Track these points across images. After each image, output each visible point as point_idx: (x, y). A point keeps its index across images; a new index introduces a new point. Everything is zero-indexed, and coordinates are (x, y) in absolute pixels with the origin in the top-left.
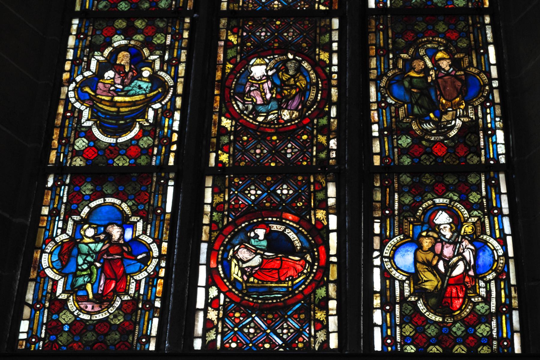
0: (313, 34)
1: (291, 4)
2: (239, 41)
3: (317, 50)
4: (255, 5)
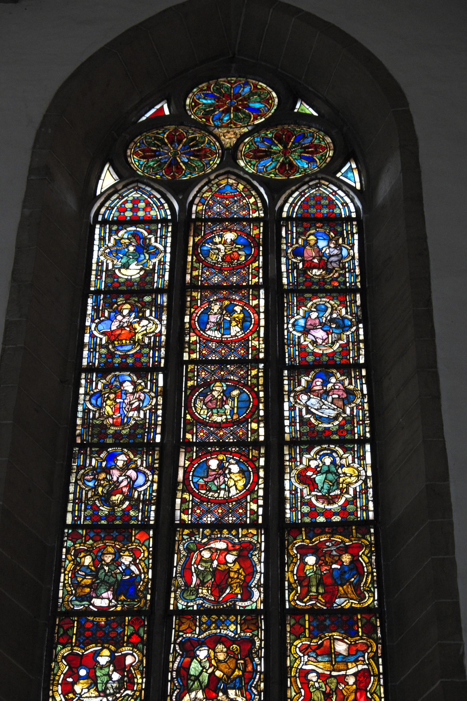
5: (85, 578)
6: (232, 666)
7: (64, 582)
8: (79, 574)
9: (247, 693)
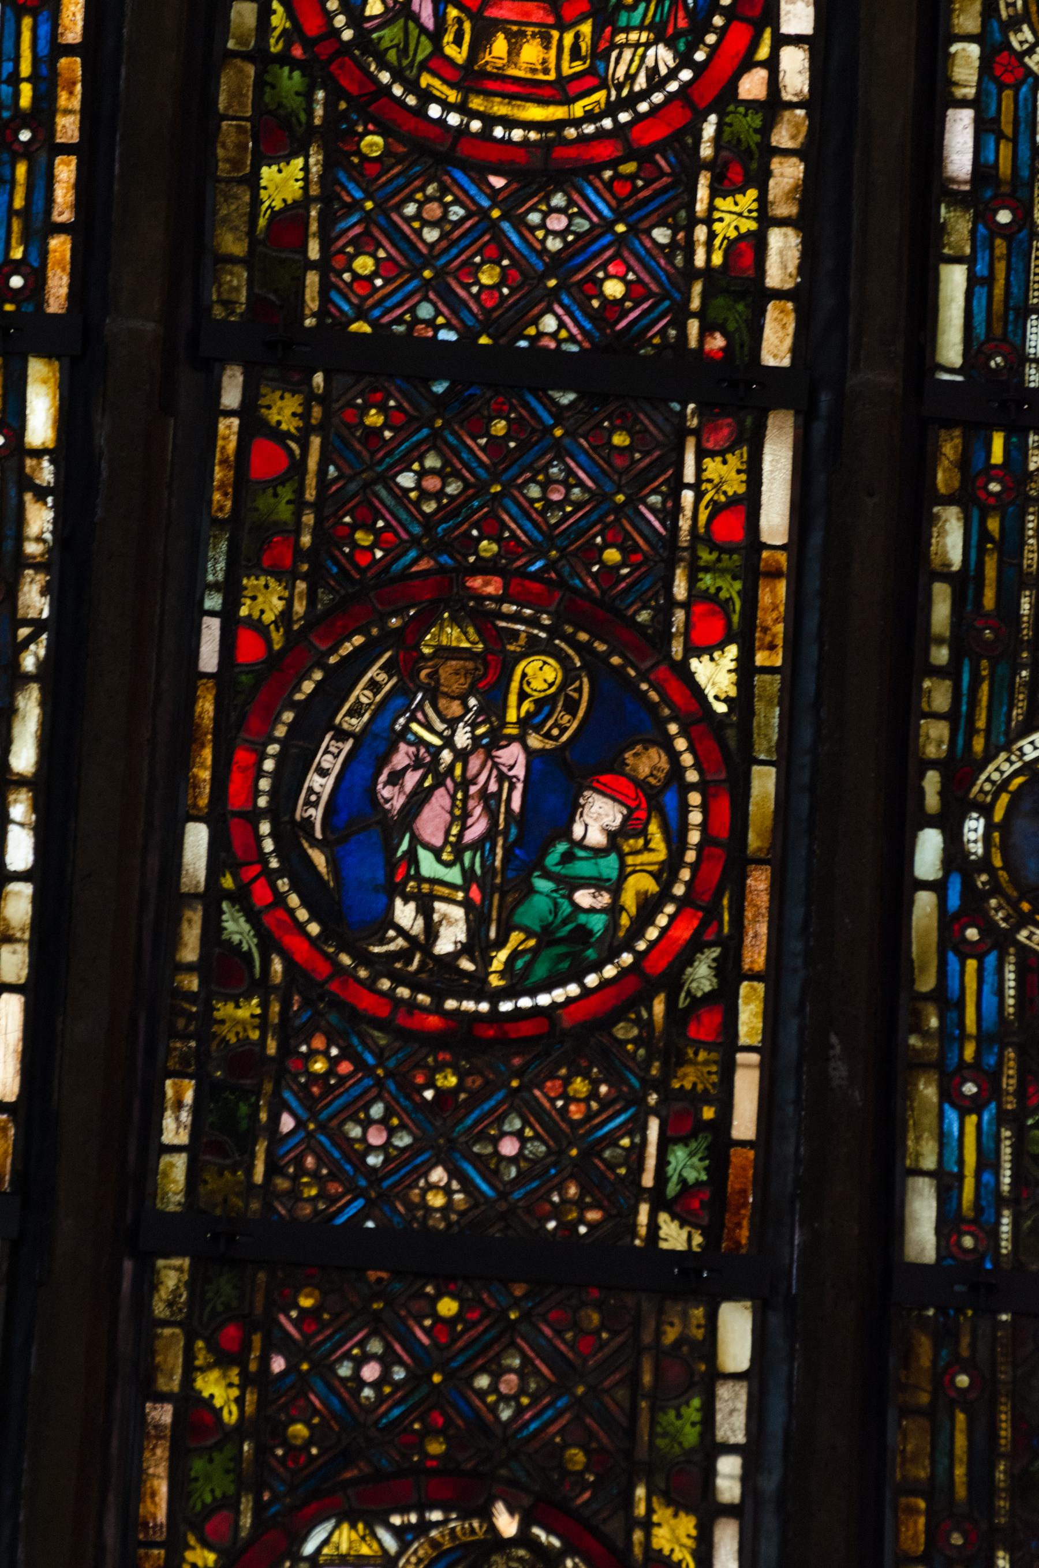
0: (621, 1393)
1: (517, 1195)
2: (249, 1409)
3: (640, 1492)
4: (335, 1188)
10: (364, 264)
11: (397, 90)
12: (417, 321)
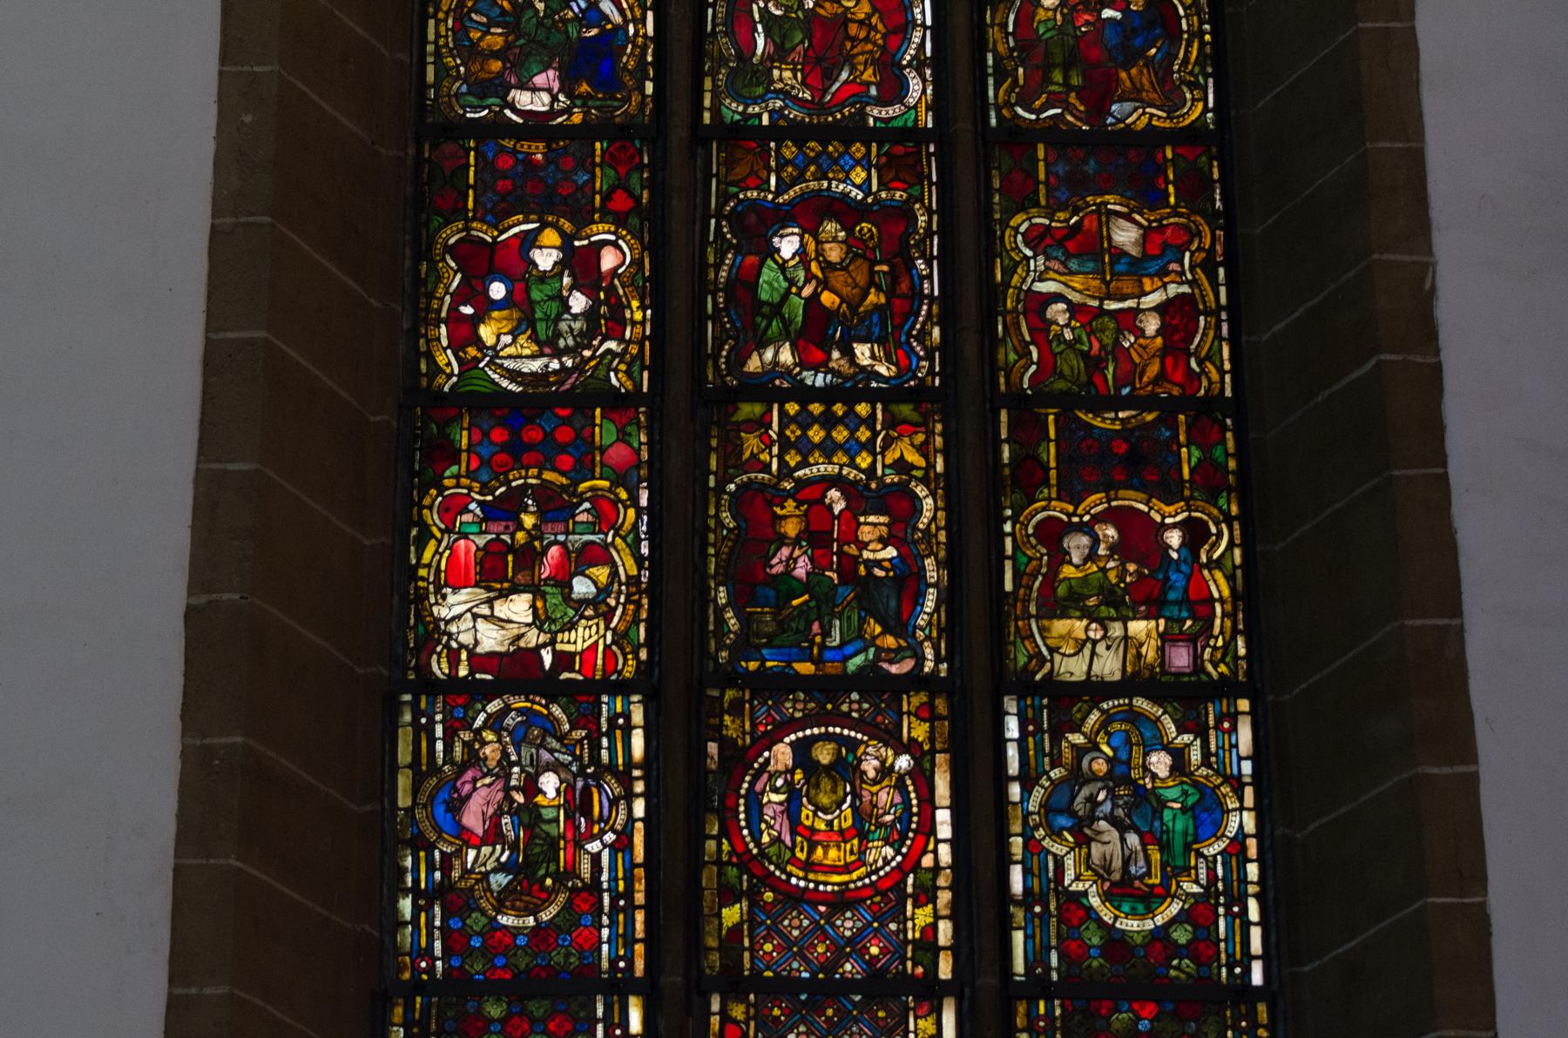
5: (488, 32)
6: (861, 279)
7: (436, 42)
8: (471, 19)
9: (900, 352)
10: (768, 947)
11: (778, 873)
12: (792, 969)
